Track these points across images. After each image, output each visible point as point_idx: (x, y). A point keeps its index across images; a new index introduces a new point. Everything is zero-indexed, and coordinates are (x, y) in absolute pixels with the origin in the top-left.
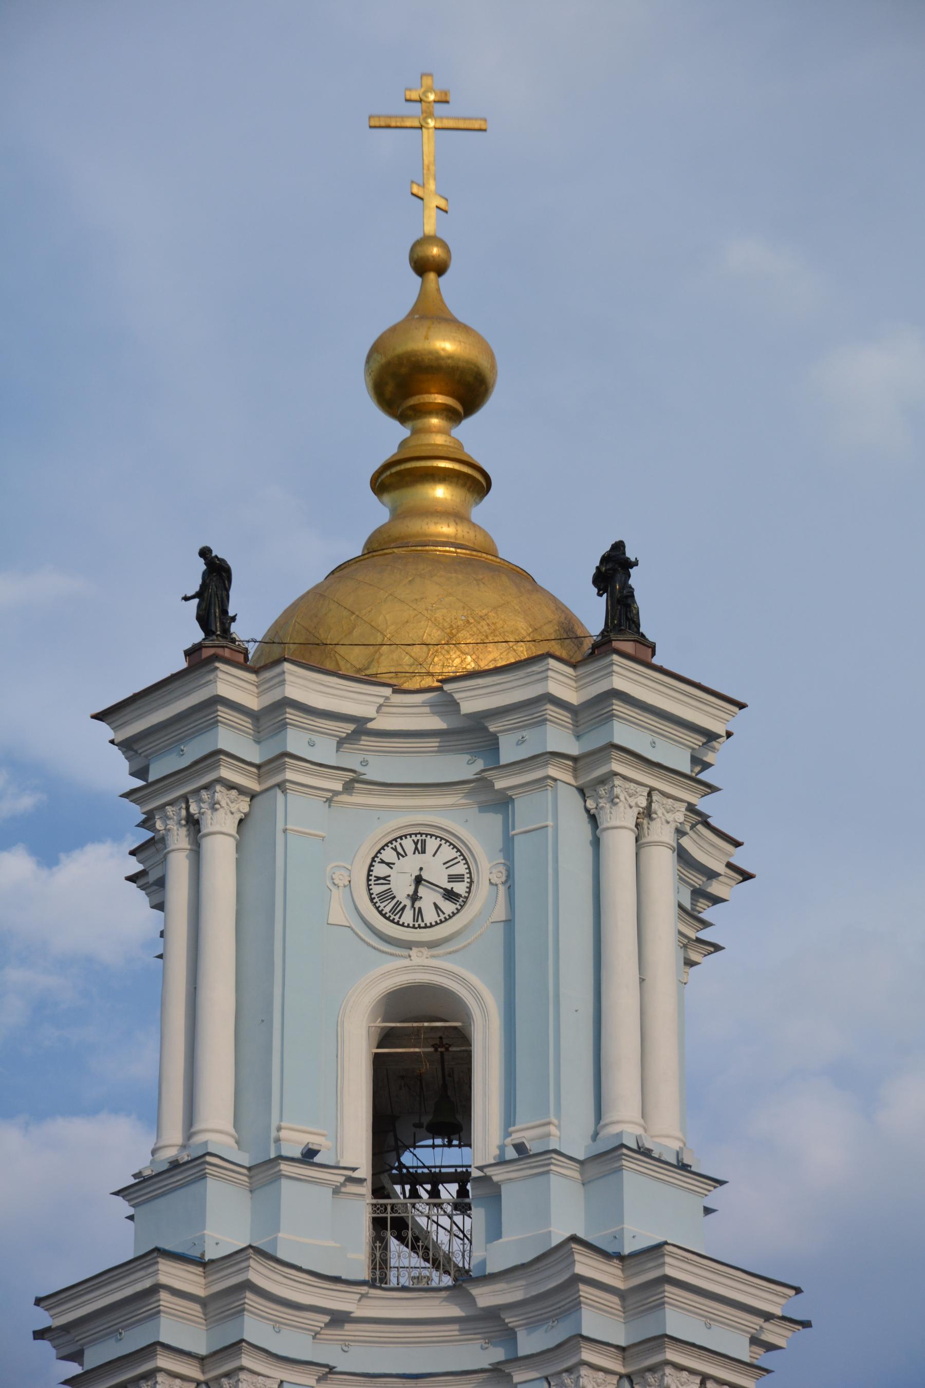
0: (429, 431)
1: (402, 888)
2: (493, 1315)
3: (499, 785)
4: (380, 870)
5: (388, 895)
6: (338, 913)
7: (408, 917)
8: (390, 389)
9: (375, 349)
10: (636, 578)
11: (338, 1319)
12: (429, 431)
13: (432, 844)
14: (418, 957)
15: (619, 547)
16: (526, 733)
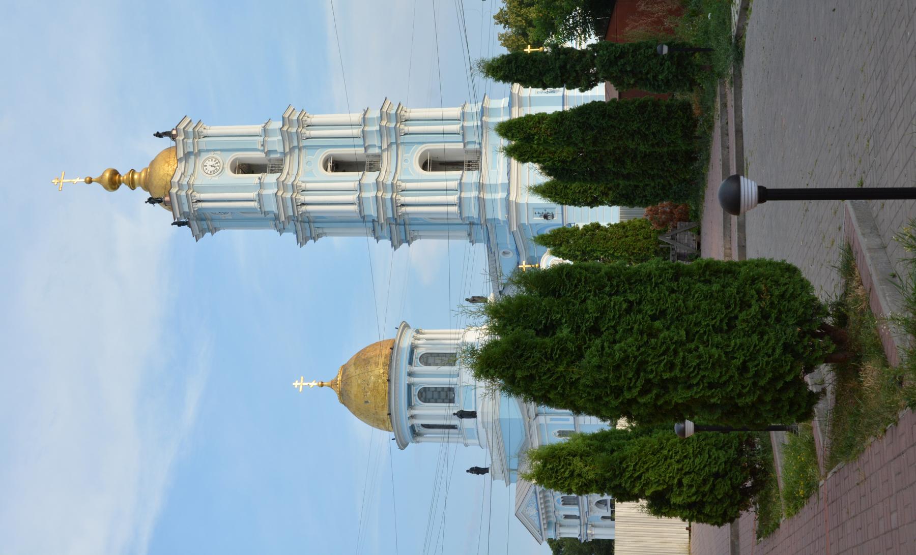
0: (123, 180)
1: (213, 169)
2: (290, 149)
3: (196, 151)
4: (209, 173)
5: (214, 171)
6: (217, 178)
7: (218, 168)
8: (114, 187)
9: (106, 188)
10: (161, 132)
11: (288, 173)
12: (123, 180)
13: (205, 164)
14: (225, 166)
15: (154, 135)
16: (188, 145)
